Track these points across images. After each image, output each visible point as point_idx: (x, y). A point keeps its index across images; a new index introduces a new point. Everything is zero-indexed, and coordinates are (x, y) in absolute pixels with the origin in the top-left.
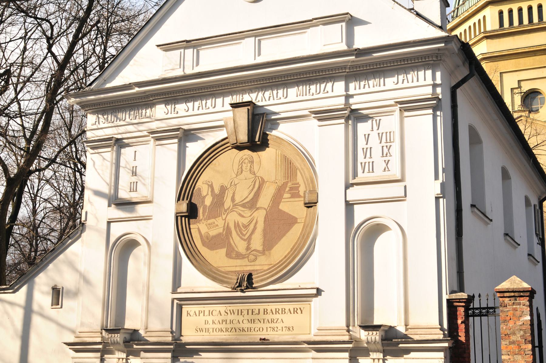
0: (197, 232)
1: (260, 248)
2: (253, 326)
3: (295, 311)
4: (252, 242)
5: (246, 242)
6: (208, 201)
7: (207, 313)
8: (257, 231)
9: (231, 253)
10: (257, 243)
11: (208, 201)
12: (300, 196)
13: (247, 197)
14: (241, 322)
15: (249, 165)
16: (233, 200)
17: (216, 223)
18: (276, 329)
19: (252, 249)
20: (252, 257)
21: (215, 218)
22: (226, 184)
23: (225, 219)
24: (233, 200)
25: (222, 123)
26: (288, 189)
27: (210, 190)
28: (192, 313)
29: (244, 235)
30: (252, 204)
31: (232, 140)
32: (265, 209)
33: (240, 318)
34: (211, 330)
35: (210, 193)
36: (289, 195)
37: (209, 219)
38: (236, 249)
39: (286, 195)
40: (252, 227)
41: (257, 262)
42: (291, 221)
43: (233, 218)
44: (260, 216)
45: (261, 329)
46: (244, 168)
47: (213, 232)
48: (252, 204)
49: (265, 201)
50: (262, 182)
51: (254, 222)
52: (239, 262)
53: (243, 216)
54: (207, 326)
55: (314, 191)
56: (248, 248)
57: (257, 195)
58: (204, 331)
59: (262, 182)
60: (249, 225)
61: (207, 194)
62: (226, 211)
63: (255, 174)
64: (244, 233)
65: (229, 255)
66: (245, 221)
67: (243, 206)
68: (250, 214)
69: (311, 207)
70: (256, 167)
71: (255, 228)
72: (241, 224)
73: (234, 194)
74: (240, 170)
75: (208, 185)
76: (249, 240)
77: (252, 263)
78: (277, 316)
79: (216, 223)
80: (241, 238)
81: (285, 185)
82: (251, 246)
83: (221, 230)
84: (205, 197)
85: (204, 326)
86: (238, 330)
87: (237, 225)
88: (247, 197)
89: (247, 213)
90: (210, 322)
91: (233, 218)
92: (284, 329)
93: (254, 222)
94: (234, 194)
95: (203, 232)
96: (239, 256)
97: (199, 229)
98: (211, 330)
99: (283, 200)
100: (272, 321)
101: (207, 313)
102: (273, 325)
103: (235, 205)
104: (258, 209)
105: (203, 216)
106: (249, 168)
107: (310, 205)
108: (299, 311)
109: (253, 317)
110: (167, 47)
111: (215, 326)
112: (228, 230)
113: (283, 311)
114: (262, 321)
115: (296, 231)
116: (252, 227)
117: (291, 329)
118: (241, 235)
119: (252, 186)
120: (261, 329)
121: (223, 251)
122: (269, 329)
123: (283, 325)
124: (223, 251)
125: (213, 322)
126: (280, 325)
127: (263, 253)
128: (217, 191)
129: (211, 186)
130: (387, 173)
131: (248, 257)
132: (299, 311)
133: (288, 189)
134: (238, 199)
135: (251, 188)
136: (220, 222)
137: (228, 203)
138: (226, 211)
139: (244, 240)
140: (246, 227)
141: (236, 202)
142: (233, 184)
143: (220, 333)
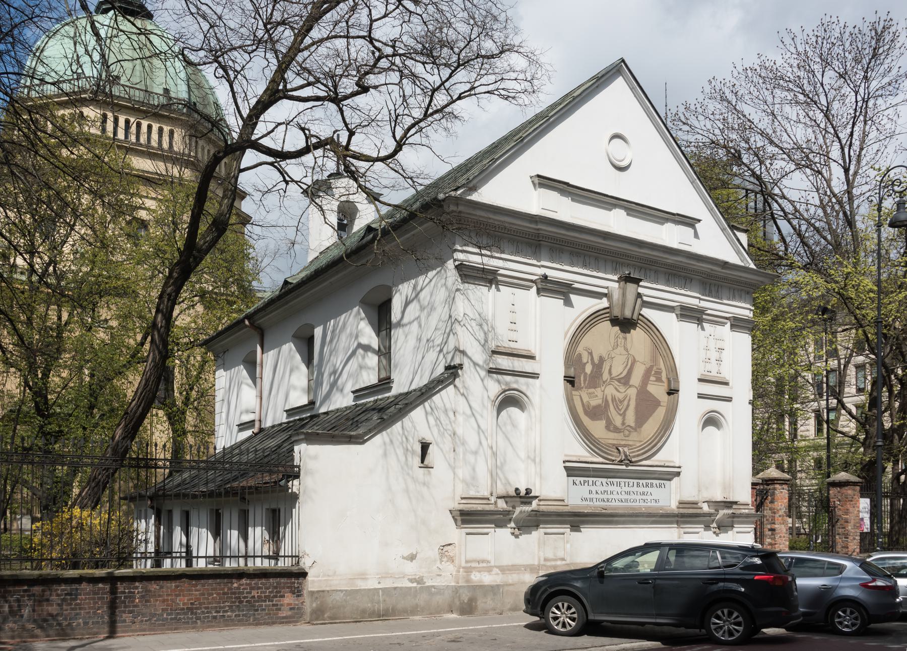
0: (579, 400)
1: (633, 424)
3: (660, 486)
4: (626, 417)
6: (588, 369)
7: (591, 483)
11: (588, 369)
12: (662, 382)
13: (621, 373)
17: (596, 393)
20: (627, 433)
22: (605, 355)
25: (605, 291)
26: (653, 372)
28: (577, 482)
29: (620, 410)
30: (625, 381)
31: (616, 312)
33: (618, 489)
34: (595, 500)
35: (590, 361)
37: (590, 388)
39: (652, 378)
40: (626, 403)
41: (630, 438)
43: (610, 391)
44: (632, 392)
47: (594, 402)
48: (625, 381)
49: (636, 379)
50: (634, 361)
51: (628, 398)
53: (619, 391)
54: (591, 496)
55: (676, 380)
56: (623, 424)
60: (624, 400)
61: (588, 362)
62: (604, 382)
64: (620, 408)
65: (608, 428)
67: (619, 380)
68: (624, 390)
69: (673, 394)
70: (629, 346)
71: (628, 406)
73: (611, 366)
76: (623, 415)
77: (627, 438)
79: (596, 393)
82: (625, 421)
85: (589, 496)
87: (614, 399)
88: (621, 373)
89: (622, 389)
90: (594, 492)
91: (610, 391)
93: (628, 398)
94: (611, 366)
95: (585, 401)
96: (617, 430)
97: (580, 396)
98: (595, 500)
101: (591, 483)
102: (644, 497)
103: (612, 379)
104: (630, 386)
105: (584, 383)
107: (673, 392)
108: (663, 486)
110: (544, 182)
111: (597, 496)
113: (652, 485)
115: (660, 413)
116: (626, 403)
118: (617, 408)
121: (603, 423)
124: (603, 423)
125: (597, 493)
126: (649, 498)
128: (596, 360)
129: (591, 354)
130: (719, 375)
132: (663, 486)
133: (653, 372)
134: (614, 373)
135: (625, 365)
136: (598, 392)
137: (606, 376)
138: (604, 382)
139: (620, 415)
140: (621, 402)
143: (602, 503)
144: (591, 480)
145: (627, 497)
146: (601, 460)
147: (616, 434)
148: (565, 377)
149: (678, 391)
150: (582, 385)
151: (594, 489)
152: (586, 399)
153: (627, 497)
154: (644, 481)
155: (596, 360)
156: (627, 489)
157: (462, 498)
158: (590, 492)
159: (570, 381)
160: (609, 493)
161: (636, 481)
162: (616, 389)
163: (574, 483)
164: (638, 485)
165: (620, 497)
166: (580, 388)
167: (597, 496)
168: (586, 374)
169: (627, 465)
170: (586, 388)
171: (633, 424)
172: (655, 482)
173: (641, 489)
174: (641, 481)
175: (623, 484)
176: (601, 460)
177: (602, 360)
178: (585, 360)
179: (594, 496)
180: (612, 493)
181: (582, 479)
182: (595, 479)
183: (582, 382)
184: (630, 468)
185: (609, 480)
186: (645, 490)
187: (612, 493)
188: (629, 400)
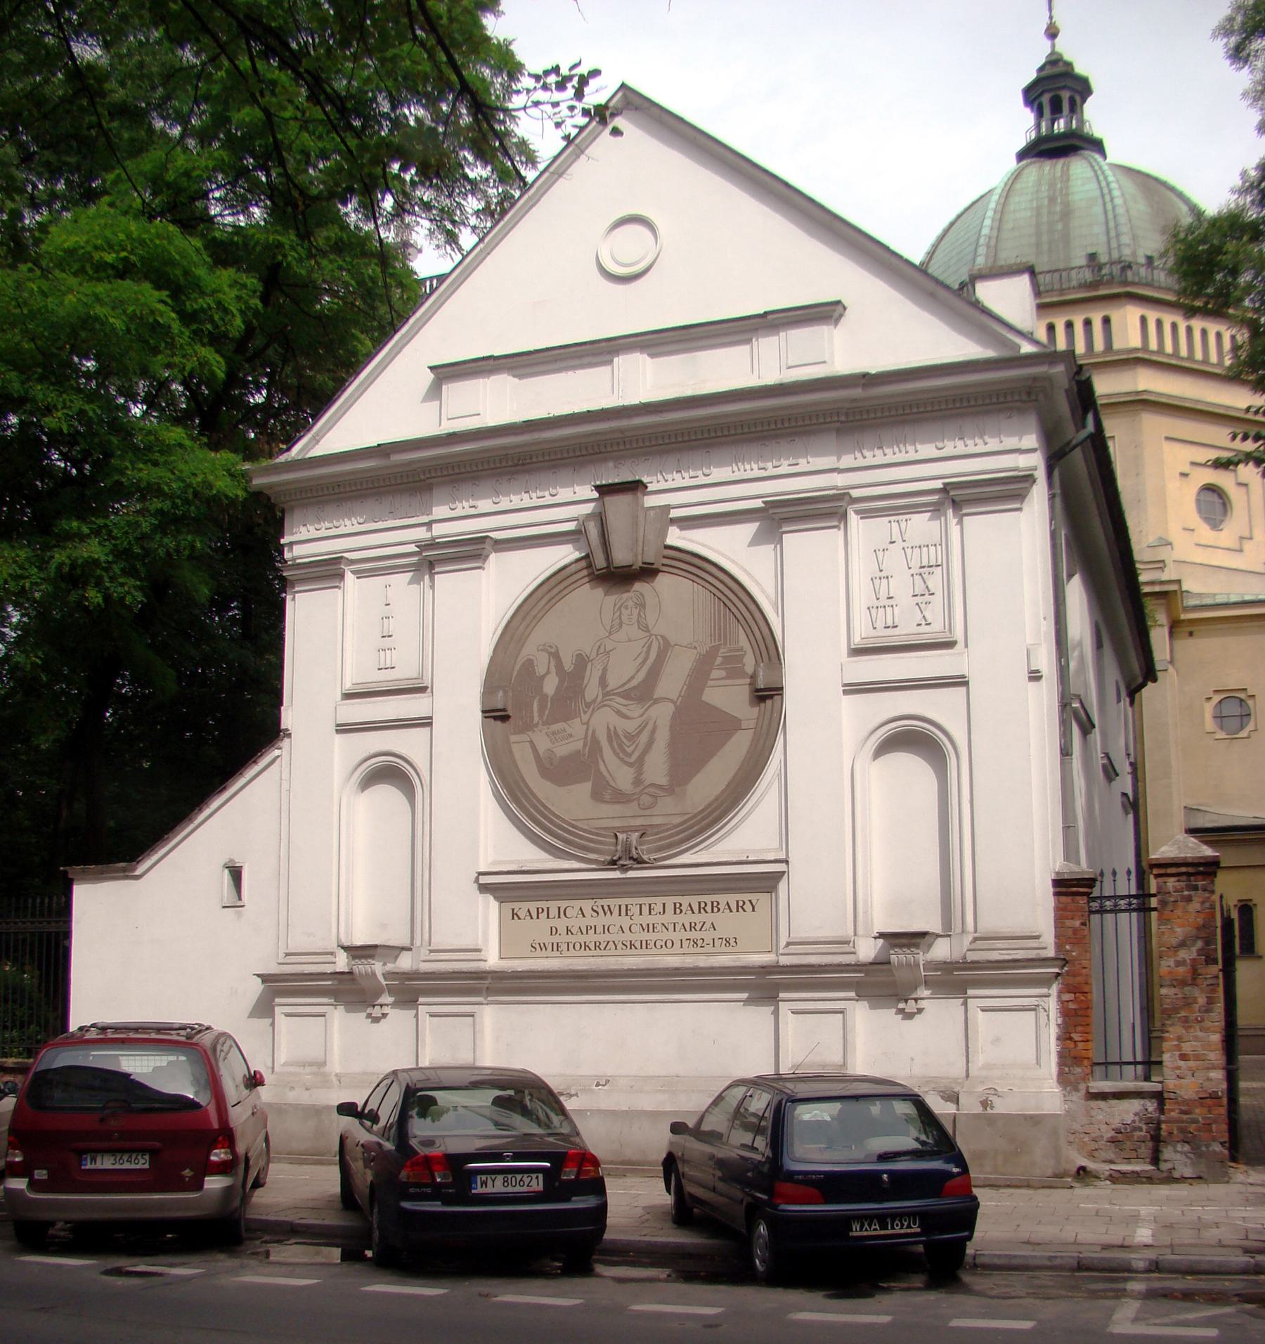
1: (663, 781)
2: (651, 936)
3: (740, 907)
4: (646, 768)
5: (632, 770)
6: (550, 685)
7: (554, 912)
8: (654, 746)
9: (603, 792)
10: (657, 768)
11: (550, 685)
13: (632, 678)
14: (626, 929)
15: (636, 612)
16: (603, 682)
18: (700, 942)
19: (646, 783)
20: (646, 800)
21: (567, 718)
23: (587, 723)
24: (603, 682)
26: (719, 660)
27: (553, 663)
28: (522, 913)
29: (629, 755)
30: (643, 692)
32: (671, 701)
33: (625, 922)
35: (553, 669)
36: (723, 673)
37: (554, 720)
38: (612, 783)
39: (715, 674)
40: (644, 738)
42: (729, 725)
43: (603, 720)
44: (662, 714)
45: (669, 944)
46: (624, 618)
47: (562, 750)
49: (672, 683)
50: (666, 647)
51: (649, 727)
52: (617, 809)
54: (556, 939)
56: (638, 781)
57: (653, 675)
58: (550, 948)
59: (666, 647)
60: (640, 732)
61: (548, 672)
62: (588, 705)
63: (648, 631)
64: (629, 750)
65: (597, 796)
66: (631, 726)
67: (626, 695)
69: (771, 697)
70: (650, 618)
72: (620, 733)
73: (605, 670)
74: (617, 621)
75: (550, 654)
77: (647, 812)
78: (703, 917)
79: (569, 731)
80: (621, 759)
81: (714, 651)
82: (644, 776)
83: (579, 745)
84: (542, 678)
85: (548, 939)
86: (620, 945)
87: (612, 735)
88: (632, 678)
89: (635, 710)
90: (562, 930)
91: (603, 720)
92: (718, 942)
93: (649, 727)
94: (605, 670)
95: (541, 750)
96: (620, 797)
97: (531, 742)
98: (564, 947)
99: (710, 683)
100: (692, 927)
101: (554, 912)
102: (693, 935)
103: (605, 695)
104: (656, 701)
105: (541, 716)
106: (635, 617)
108: (748, 907)
109: (651, 920)
111: (570, 938)
112: (594, 746)
113: (715, 907)
114: (671, 928)
116: (644, 738)
117: (732, 942)
118: (621, 753)
119: (643, 655)
120: (669, 944)
121: (586, 788)
122: (685, 943)
123: (716, 935)
124: (586, 788)
127: (670, 790)
128: (568, 665)
129: (555, 655)
131: (638, 799)
132: (748, 907)
133: (719, 660)
134: (613, 682)
135: (640, 660)
136: (576, 727)
137: (592, 691)
138: (588, 705)
139: (630, 765)
140: (632, 738)
141: (609, 689)
142: (602, 650)
144: (553, 906)
145: (645, 936)
146: (576, 865)
147: (617, 807)
148: (483, 712)
149: (782, 689)
150: (536, 719)
151: (561, 924)
152: (543, 744)
153: (645, 936)
154: (694, 900)
155: (568, 665)
156: (646, 919)
157: (287, 954)
158: (554, 931)
159: (495, 715)
160: (600, 929)
161: (670, 901)
162: (619, 713)
163: (514, 914)
164: (677, 908)
165: (627, 937)
166: (528, 727)
167: (570, 938)
168: (544, 698)
169: (624, 868)
170: (544, 724)
171: (663, 781)
172: (722, 899)
173: (686, 918)
174: (685, 901)
175: (636, 910)
176: (576, 865)
177: (582, 662)
178: (541, 669)
179: (563, 938)
180: (606, 929)
181: (533, 906)
182: (563, 904)
183: (536, 714)
184: (631, 874)
185: (600, 902)
186: (698, 918)
187: (606, 929)
188: (654, 730)
